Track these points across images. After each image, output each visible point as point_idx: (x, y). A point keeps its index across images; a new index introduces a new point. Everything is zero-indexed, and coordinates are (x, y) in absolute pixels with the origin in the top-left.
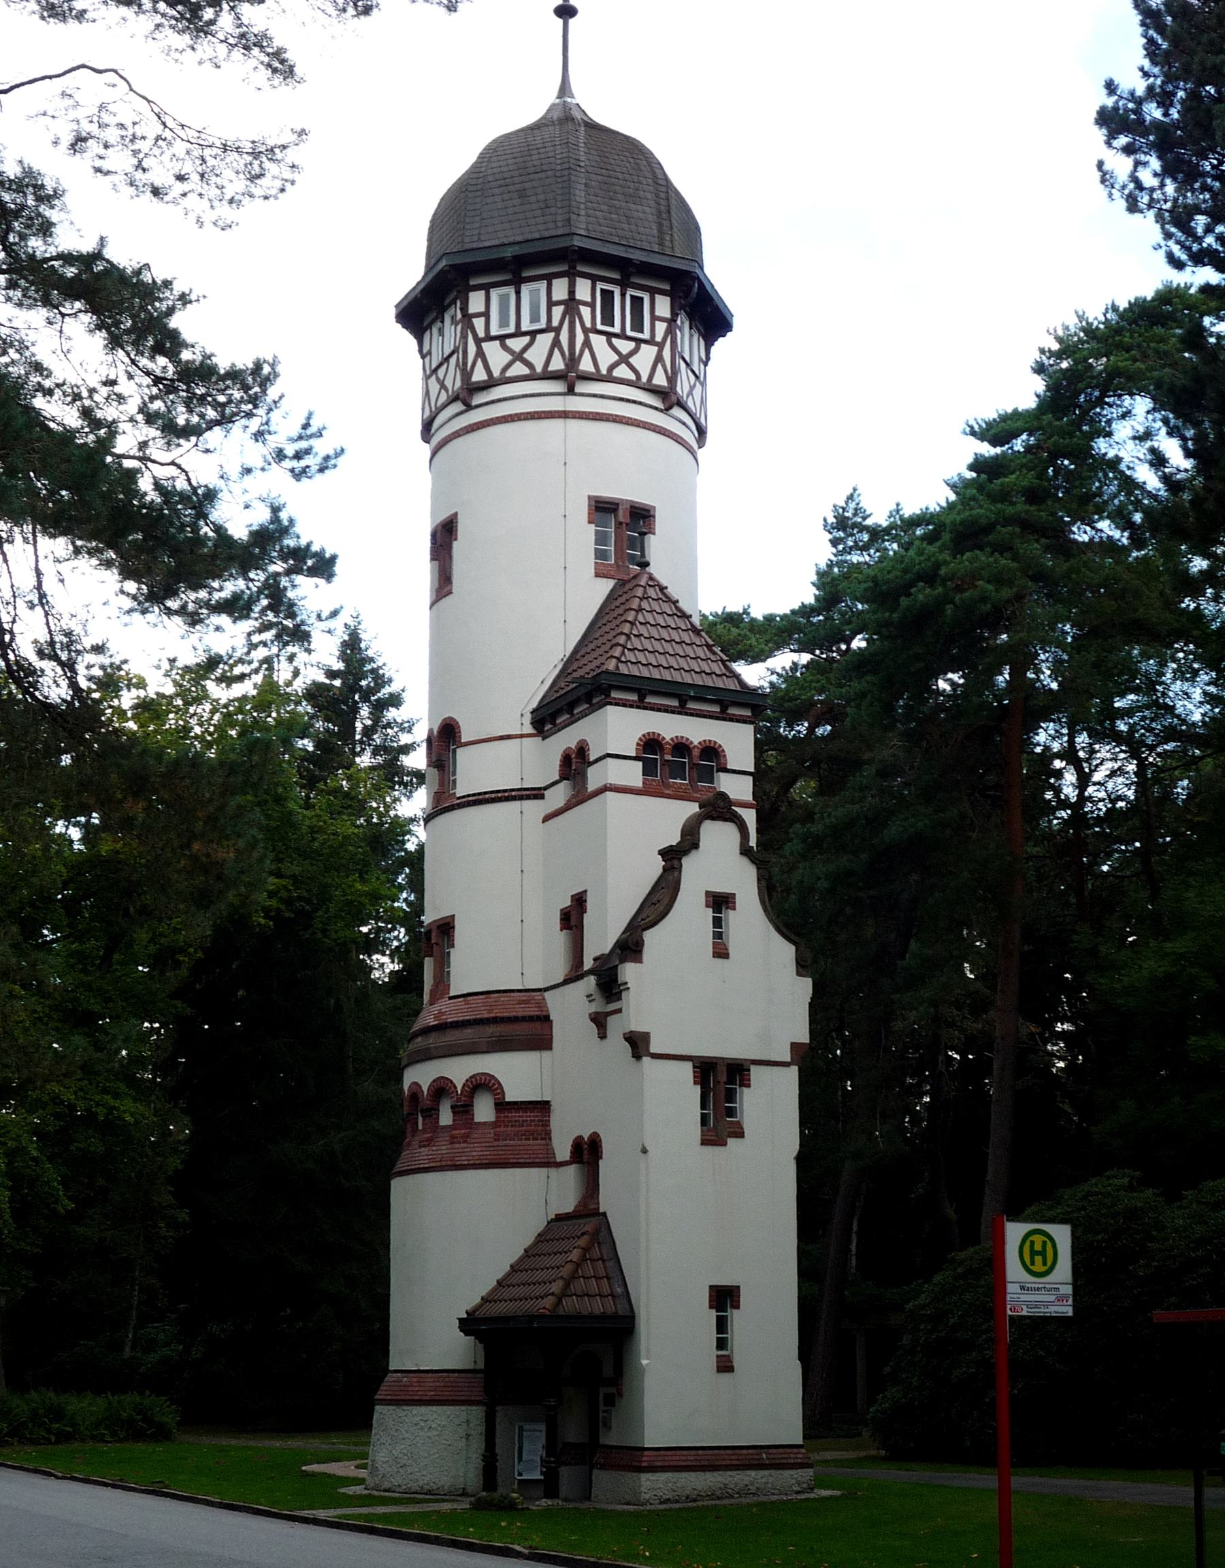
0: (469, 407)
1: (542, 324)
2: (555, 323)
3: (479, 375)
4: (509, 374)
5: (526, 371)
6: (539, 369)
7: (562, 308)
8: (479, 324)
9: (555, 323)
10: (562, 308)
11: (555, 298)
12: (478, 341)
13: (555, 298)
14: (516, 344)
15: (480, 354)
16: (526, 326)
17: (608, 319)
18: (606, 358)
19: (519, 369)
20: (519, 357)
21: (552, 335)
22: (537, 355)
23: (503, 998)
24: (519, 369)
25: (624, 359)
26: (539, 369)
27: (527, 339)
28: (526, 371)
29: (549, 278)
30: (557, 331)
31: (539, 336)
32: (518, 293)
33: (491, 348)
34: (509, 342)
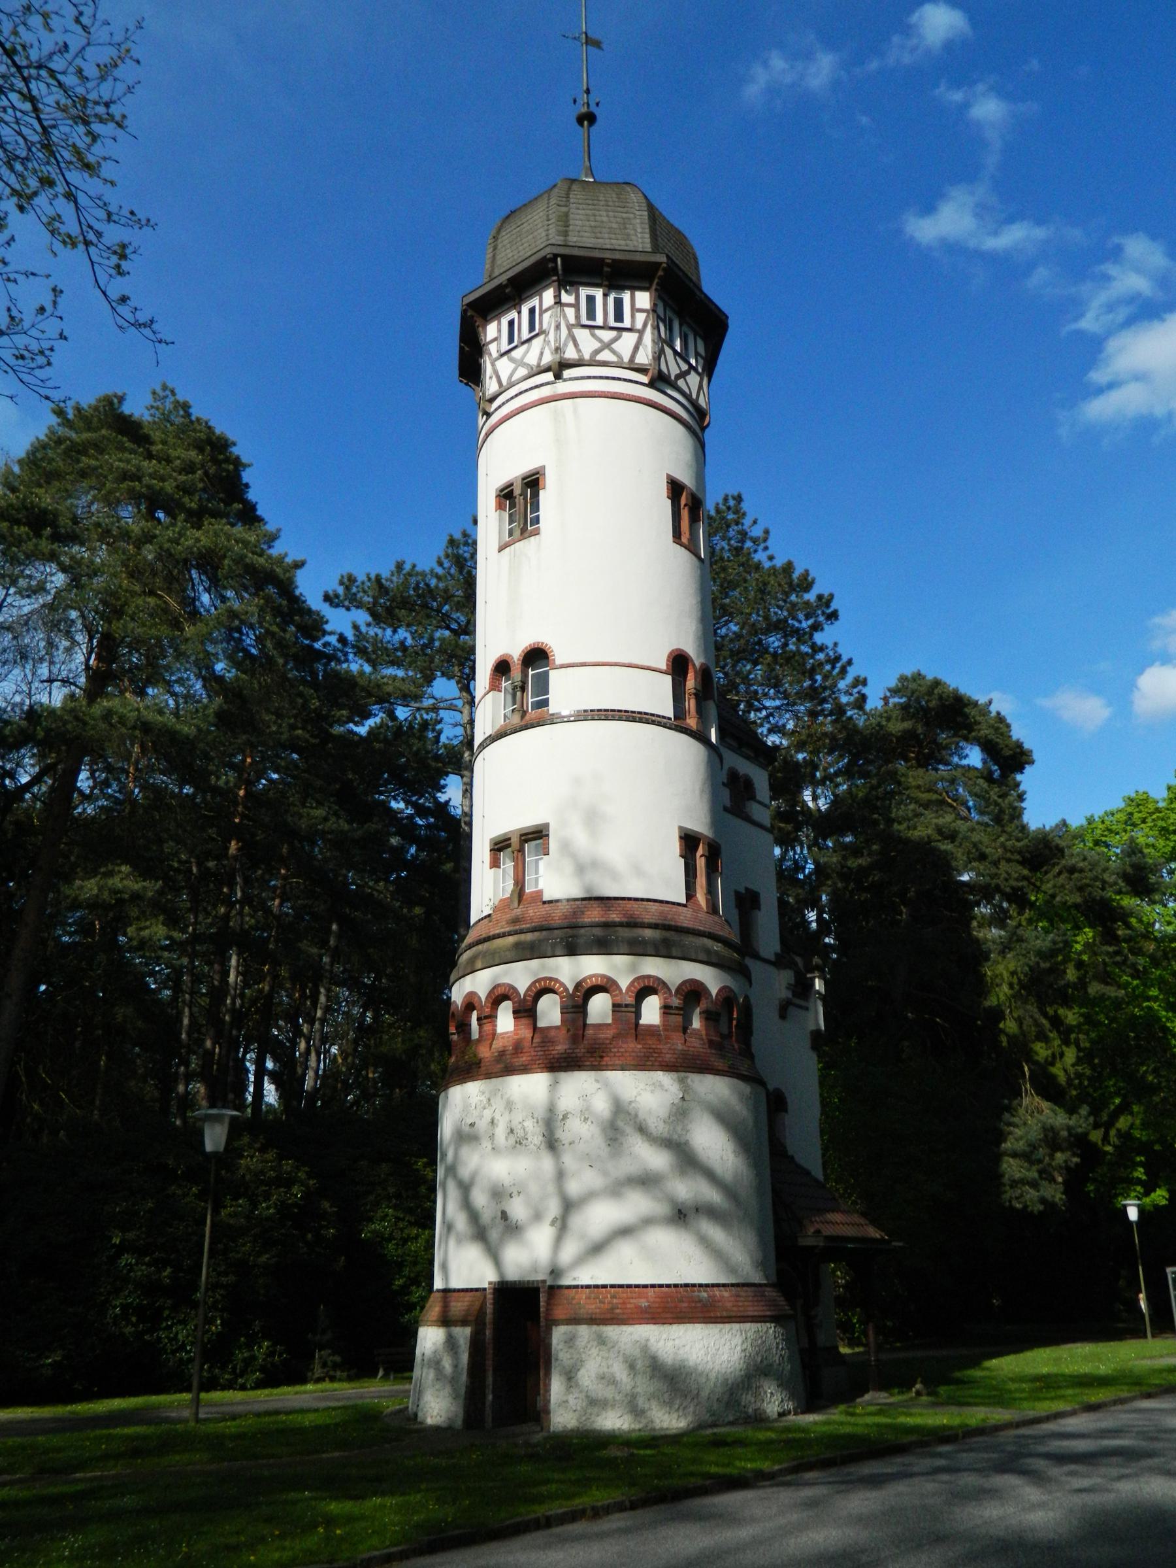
0: (558, 376)
1: (627, 323)
3: (570, 354)
4: (600, 357)
7: (644, 315)
9: (639, 326)
10: (644, 315)
11: (638, 305)
12: (570, 327)
13: (638, 305)
14: (607, 335)
16: (612, 323)
17: (591, 314)
18: (587, 343)
19: (606, 356)
20: (607, 346)
21: (636, 335)
23: (635, 905)
25: (607, 346)
26: (626, 359)
27: (614, 333)
29: (634, 289)
30: (641, 333)
31: (625, 334)
32: (605, 295)
33: (582, 335)
34: (598, 332)
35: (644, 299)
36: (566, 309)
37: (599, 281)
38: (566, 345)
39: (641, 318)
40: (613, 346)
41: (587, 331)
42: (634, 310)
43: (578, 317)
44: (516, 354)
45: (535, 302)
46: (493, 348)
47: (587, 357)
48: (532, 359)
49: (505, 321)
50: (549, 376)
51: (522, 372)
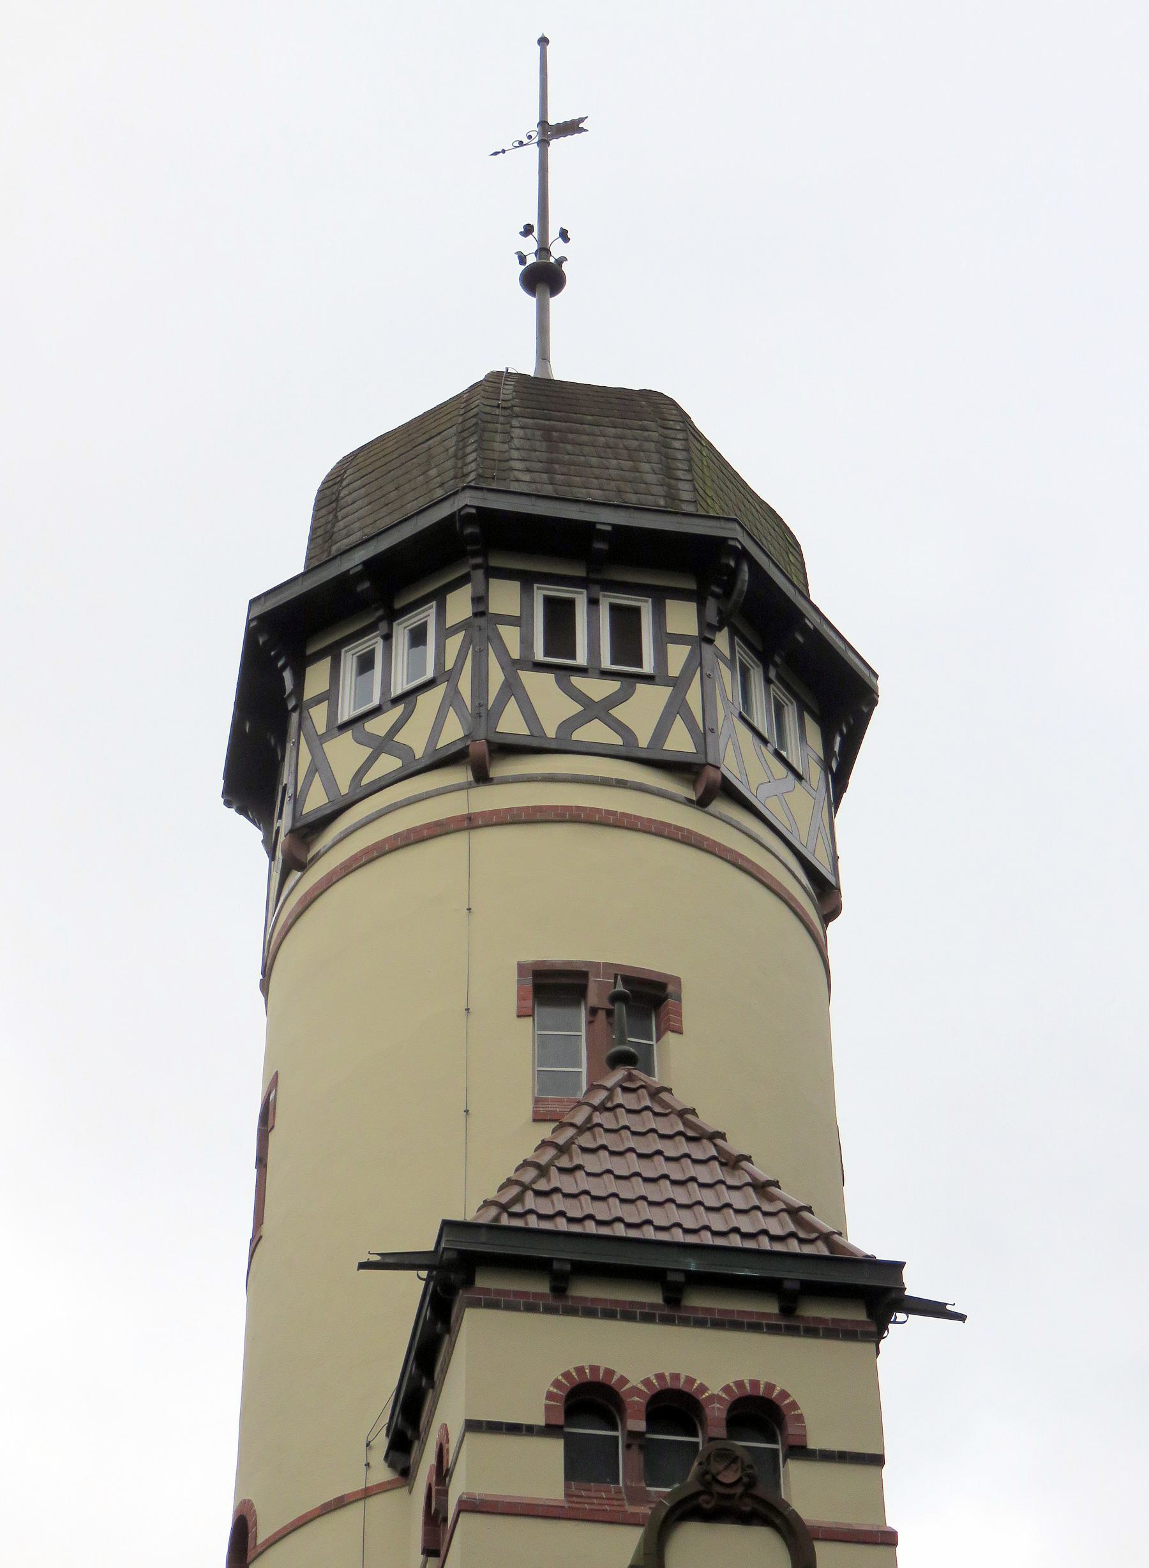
0: (482, 777)
2: (674, 670)
3: (511, 723)
4: (581, 735)
5: (615, 739)
6: (643, 742)
7: (687, 649)
8: (511, 636)
10: (687, 649)
12: (512, 666)
14: (598, 689)
15: (512, 687)
19: (595, 732)
22: (643, 710)
24: (595, 732)
26: (643, 742)
27: (614, 686)
28: (615, 739)
30: (679, 685)
31: (640, 687)
32: (593, 602)
35: (683, 617)
36: (502, 629)
37: (580, 572)
38: (501, 702)
39: (678, 656)
40: (616, 712)
41: (549, 678)
42: (663, 639)
43: (527, 643)
44: (378, 726)
45: (428, 615)
46: (319, 716)
47: (551, 732)
48: (416, 737)
49: (349, 661)
50: (460, 775)
51: (388, 764)
